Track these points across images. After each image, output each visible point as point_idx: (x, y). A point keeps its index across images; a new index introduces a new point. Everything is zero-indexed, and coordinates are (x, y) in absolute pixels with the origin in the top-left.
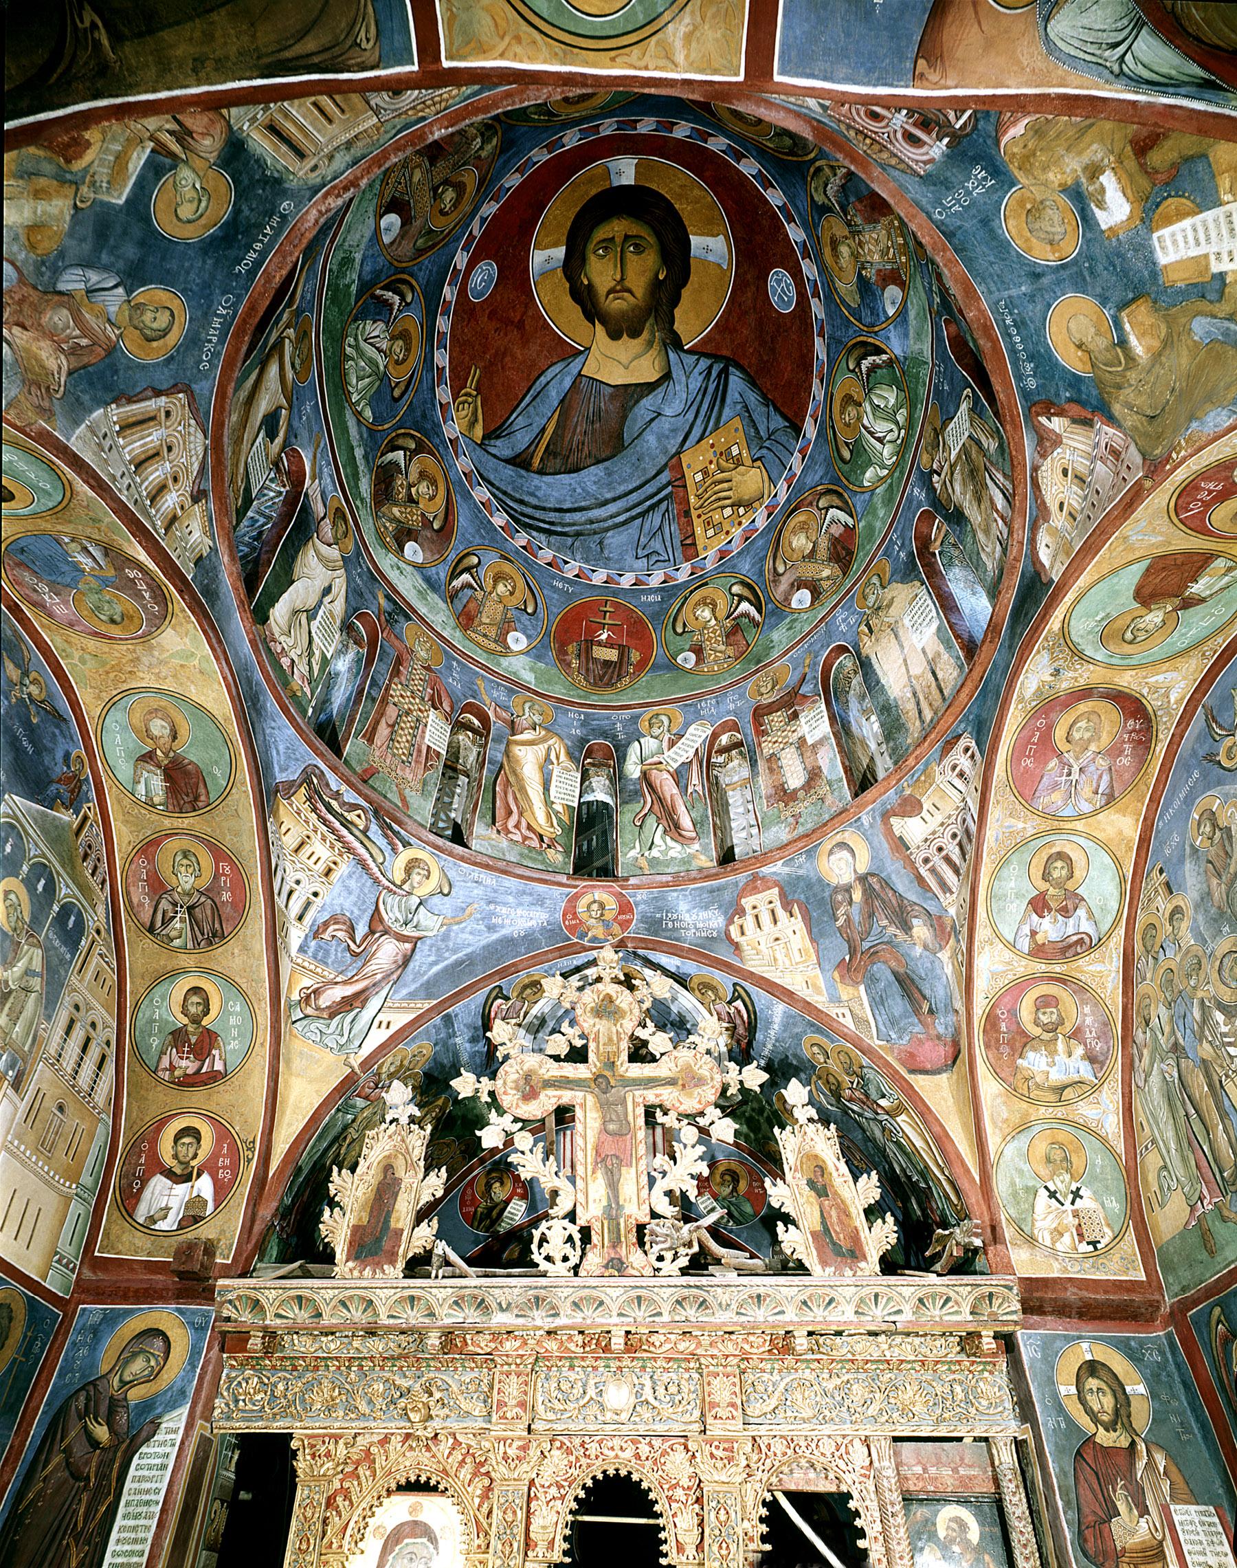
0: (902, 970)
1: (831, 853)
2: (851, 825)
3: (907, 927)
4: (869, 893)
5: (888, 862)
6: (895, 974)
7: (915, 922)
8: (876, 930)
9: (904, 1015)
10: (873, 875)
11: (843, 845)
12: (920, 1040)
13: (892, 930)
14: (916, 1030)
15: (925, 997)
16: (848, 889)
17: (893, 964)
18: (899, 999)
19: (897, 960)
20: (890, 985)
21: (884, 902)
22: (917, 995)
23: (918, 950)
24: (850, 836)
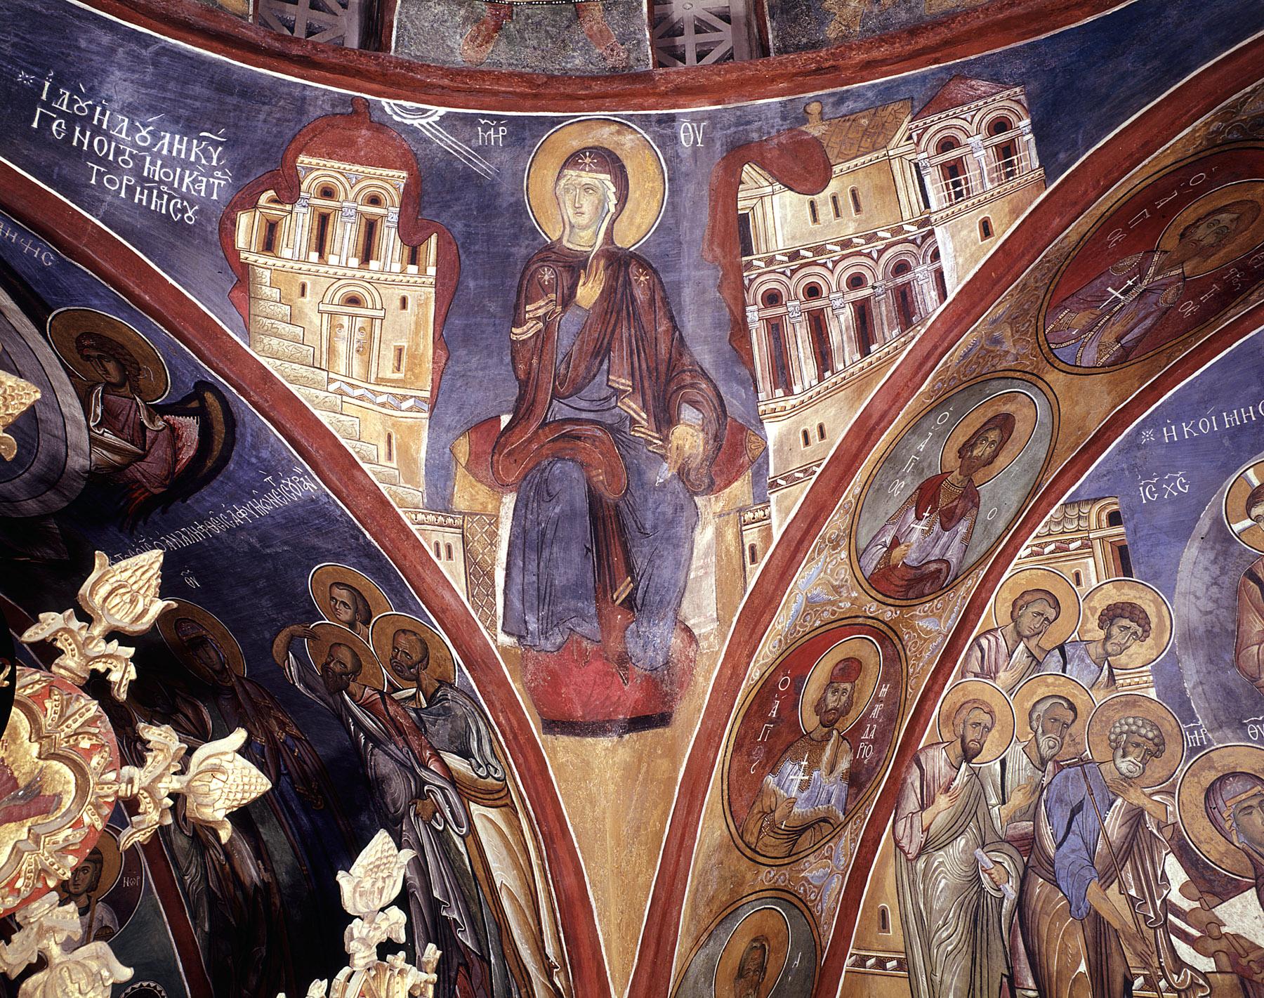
0: (610, 496)
1: (573, 160)
2: (645, 121)
3: (665, 419)
4: (616, 300)
5: (689, 258)
6: (594, 499)
7: (688, 414)
8: (597, 389)
9: (574, 590)
10: (644, 264)
11: (609, 161)
12: (582, 653)
13: (632, 406)
14: (585, 628)
15: (630, 570)
16: (575, 266)
17: (600, 477)
18: (576, 553)
19: (612, 473)
20: (571, 516)
21: (641, 339)
22: (617, 559)
23: (665, 472)
24: (631, 144)
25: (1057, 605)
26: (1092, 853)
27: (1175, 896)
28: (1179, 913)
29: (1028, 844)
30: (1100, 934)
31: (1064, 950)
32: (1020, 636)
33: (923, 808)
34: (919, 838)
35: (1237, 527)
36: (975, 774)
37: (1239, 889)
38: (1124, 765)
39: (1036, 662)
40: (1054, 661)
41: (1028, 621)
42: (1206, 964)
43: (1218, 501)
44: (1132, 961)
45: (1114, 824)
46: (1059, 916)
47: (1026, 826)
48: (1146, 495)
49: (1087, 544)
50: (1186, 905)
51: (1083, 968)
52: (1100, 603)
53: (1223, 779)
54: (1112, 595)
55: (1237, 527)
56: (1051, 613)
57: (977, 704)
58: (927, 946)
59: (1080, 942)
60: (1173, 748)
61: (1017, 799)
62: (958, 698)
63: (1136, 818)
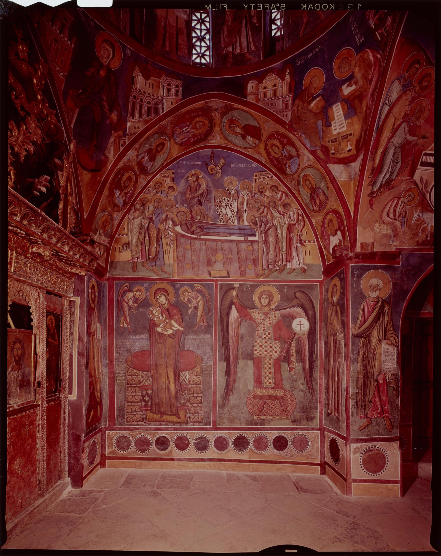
25: (162, 185)
26: (160, 220)
27: (170, 226)
28: (170, 228)
29: (151, 219)
30: (159, 231)
31: (153, 233)
32: (155, 188)
33: (134, 213)
34: (133, 217)
35: (189, 179)
36: (144, 208)
37: (178, 225)
38: (167, 209)
39: (157, 193)
40: (160, 193)
41: (157, 187)
42: (172, 234)
43: (188, 174)
44: (163, 234)
45: (164, 216)
46: (153, 228)
47: (151, 216)
48: (178, 171)
49: (168, 176)
50: (171, 227)
51: (156, 235)
52: (168, 186)
53: (179, 212)
54: (170, 185)
55: (189, 179)
56: (161, 186)
57: (146, 198)
58: (131, 234)
59: (156, 232)
60: (174, 207)
61: (150, 212)
62: (143, 197)
63: (167, 216)
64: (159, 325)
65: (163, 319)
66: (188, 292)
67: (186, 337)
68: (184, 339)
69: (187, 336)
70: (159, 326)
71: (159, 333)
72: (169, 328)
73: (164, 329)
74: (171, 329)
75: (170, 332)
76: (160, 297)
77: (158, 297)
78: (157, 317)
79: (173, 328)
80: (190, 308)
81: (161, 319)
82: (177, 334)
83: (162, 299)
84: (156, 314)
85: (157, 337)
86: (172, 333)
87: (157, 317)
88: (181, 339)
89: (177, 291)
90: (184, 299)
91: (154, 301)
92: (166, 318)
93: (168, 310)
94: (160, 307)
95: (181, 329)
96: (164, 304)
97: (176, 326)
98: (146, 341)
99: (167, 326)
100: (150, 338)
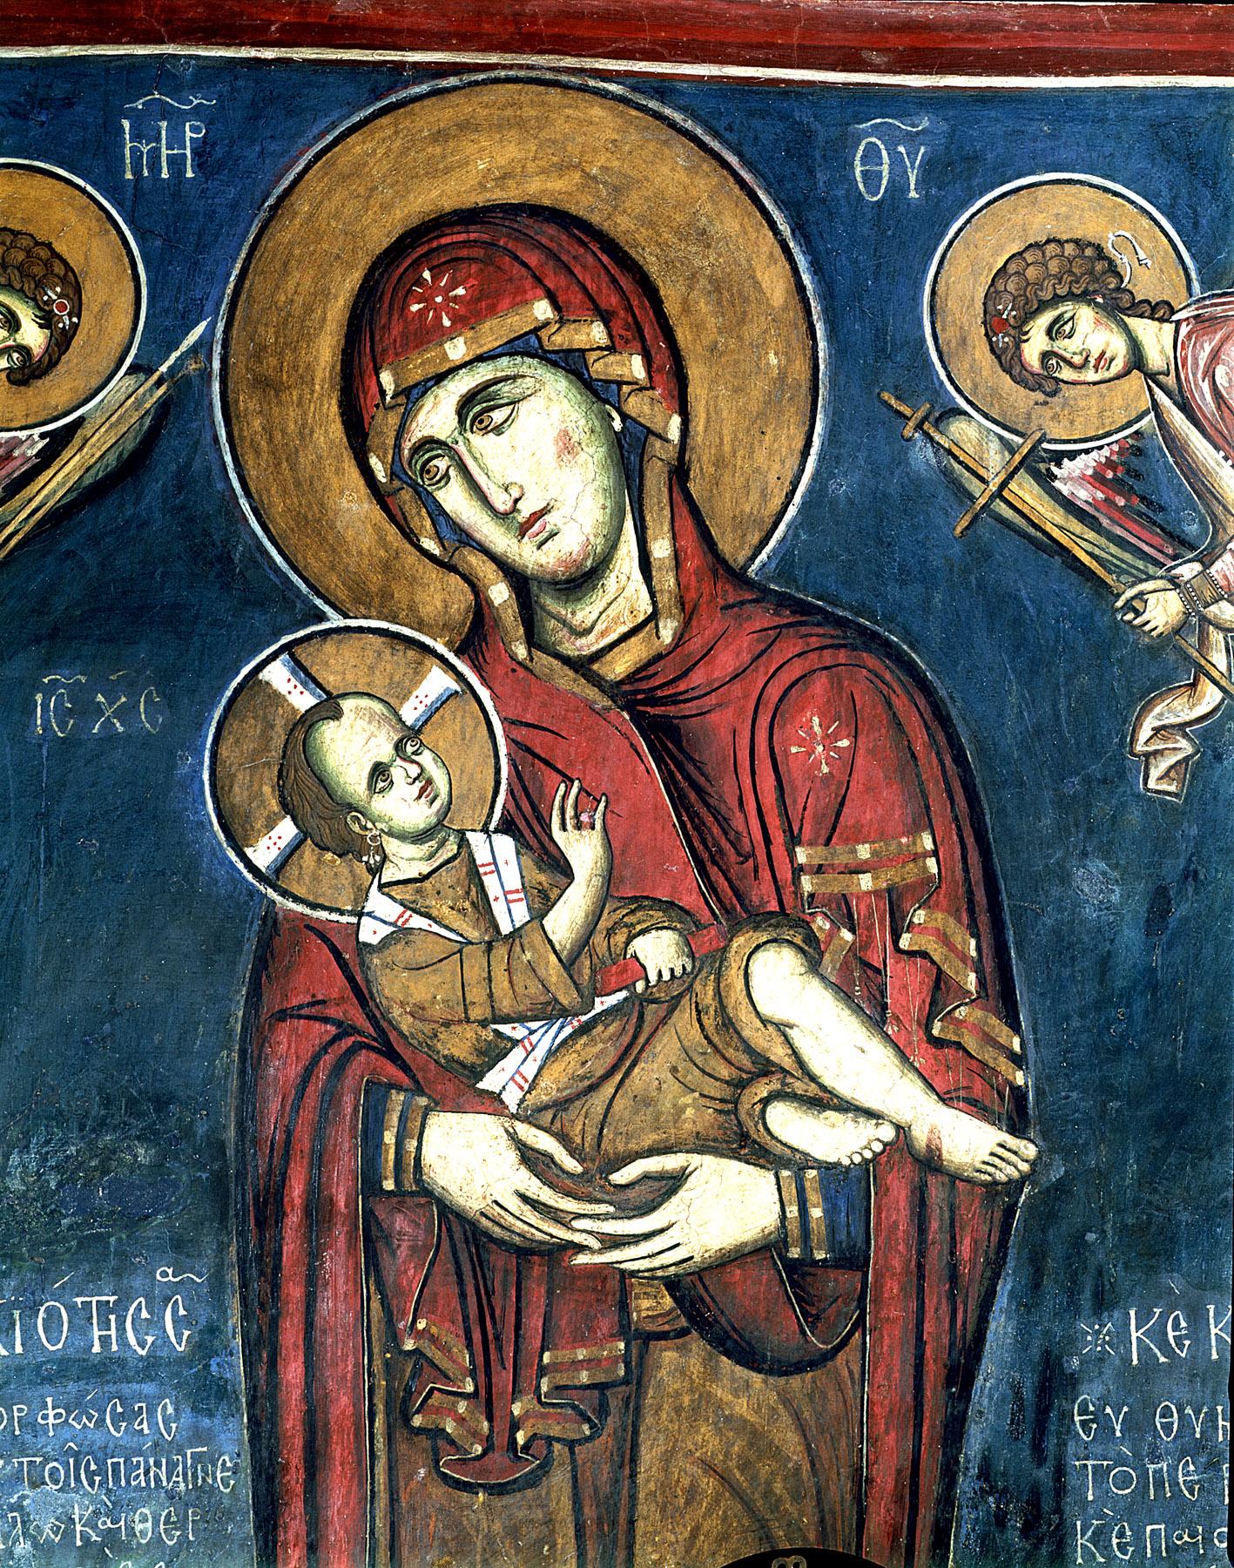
64: (459, 1045)
65: (565, 921)
66: (1120, 305)
67: (1092, 1335)
68: (1051, 1383)
69: (1103, 1303)
70: (461, 1086)
71: (467, 1239)
72: (696, 1116)
73: (593, 1156)
74: (746, 1144)
75: (724, 1208)
76: (476, 410)
77: (437, 416)
78: (406, 861)
79: (788, 1124)
80: (1169, 663)
81: (510, 915)
82: (891, 1256)
83: (535, 463)
84: (401, 807)
85: (436, 1333)
86: (768, 1249)
87: (406, 861)
88: (962, 1373)
89: (862, 277)
90: (1039, 463)
91: (353, 507)
92: (625, 898)
93: (654, 709)
94: (476, 637)
95: (970, 1142)
96: (583, 579)
97: (864, 1086)
98: (166, 1416)
99: (650, 1073)
100: (262, 1348)
